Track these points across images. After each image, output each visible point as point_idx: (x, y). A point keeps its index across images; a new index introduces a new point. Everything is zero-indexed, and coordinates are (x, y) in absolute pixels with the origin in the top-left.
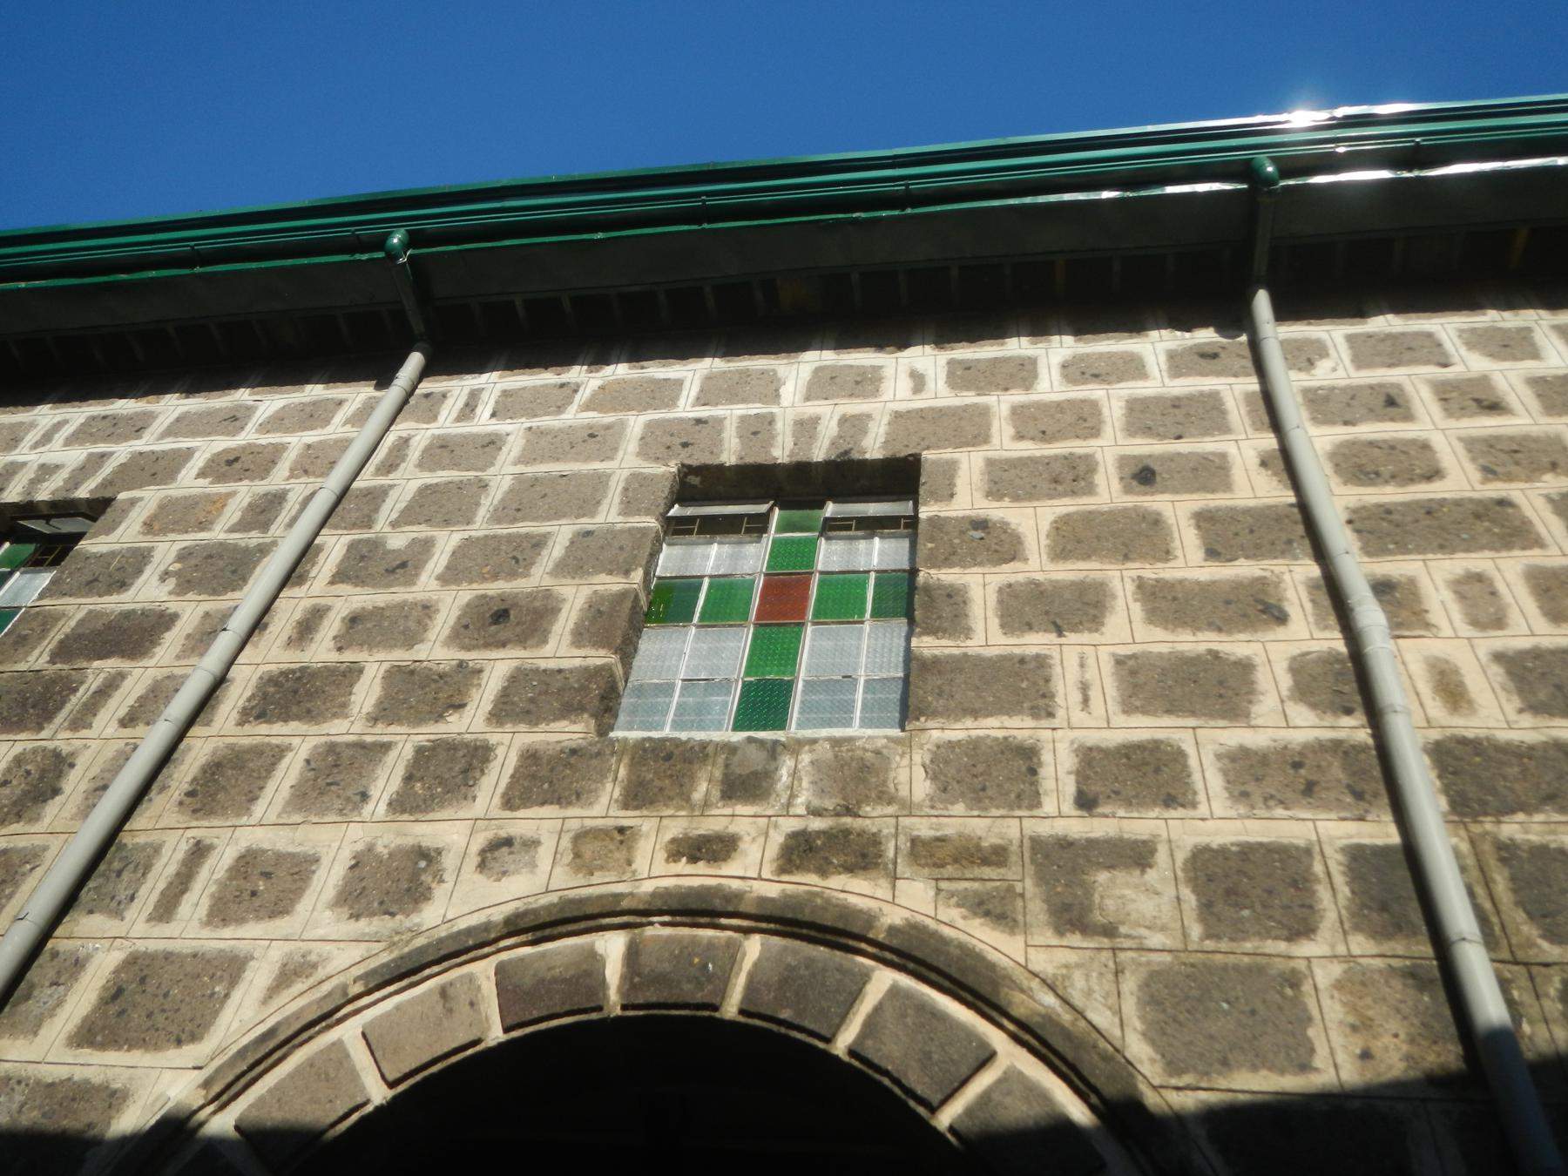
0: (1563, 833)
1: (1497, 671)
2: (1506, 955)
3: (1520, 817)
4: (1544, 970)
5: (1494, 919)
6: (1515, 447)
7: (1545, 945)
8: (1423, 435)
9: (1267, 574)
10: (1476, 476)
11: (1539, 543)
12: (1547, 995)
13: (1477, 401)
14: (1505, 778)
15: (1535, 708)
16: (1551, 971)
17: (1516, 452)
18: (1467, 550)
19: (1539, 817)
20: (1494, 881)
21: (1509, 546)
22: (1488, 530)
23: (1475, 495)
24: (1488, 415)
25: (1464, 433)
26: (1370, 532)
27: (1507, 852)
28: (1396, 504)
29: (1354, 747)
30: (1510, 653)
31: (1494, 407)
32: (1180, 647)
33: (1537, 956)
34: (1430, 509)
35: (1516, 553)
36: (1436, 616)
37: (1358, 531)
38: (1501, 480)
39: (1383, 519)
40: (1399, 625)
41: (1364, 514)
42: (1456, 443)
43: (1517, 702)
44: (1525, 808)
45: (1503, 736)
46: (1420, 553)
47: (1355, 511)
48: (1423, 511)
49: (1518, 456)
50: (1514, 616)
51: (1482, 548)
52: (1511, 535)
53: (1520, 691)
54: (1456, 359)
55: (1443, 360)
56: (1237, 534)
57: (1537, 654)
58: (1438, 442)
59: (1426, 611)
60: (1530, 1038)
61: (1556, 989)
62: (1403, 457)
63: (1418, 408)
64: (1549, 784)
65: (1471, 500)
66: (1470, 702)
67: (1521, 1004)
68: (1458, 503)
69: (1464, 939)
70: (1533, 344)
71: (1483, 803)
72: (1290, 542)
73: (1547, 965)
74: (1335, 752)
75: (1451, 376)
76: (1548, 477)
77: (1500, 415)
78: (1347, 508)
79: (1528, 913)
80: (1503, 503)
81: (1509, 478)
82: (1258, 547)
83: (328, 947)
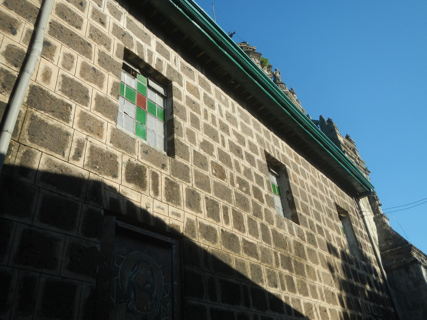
0: (49, 120)
1: (60, 79)
2: (17, 140)
3: (43, 112)
4: (24, 146)
5: (19, 131)
6: (101, 35)
7: (28, 141)
8: (83, 17)
9: (18, 20)
10: (88, 35)
11: (90, 58)
12: (20, 152)
13: (100, 19)
14: (45, 102)
15: (63, 91)
16: (25, 147)
17: (100, 36)
18: (74, 49)
19: (47, 114)
20: (26, 123)
21: (83, 55)
22: (81, 48)
23: (84, 39)
24: (100, 24)
25: (92, 24)
26: (54, 30)
27: (33, 118)
28: (65, 27)
29: (11, 75)
30: (67, 77)
31: (103, 23)
33: (24, 142)
34: (72, 34)
35: (84, 57)
36: (56, 58)
37: (51, 27)
38: (92, 39)
39: (59, 28)
40: (45, 55)
41: (55, 24)
42: (89, 24)
43: (60, 88)
44: (45, 111)
45: (51, 93)
46: (62, 42)
47: (53, 22)
48: (70, 34)
49: (100, 37)
50: (73, 70)
51: (77, 51)
52: (86, 52)
53: (63, 86)
54: (103, 7)
55: (100, 5)
56: (17, 4)
57: (72, 80)
58: (85, 21)
59: (54, 56)
60: (9, 159)
61: (23, 151)
62: (74, 18)
63: (86, 10)
64: (54, 108)
65: (83, 39)
66: (49, 82)
67: (13, 151)
68: (79, 38)
69: (7, 131)
70: (120, 17)
71: (36, 105)
72: (31, 17)
73: (25, 145)
74: (5, 73)
75: (99, 9)
76: (103, 46)
77: (103, 26)
78: (52, 20)
79: (29, 133)
80: (89, 44)
81: (94, 40)
82: (21, 11)
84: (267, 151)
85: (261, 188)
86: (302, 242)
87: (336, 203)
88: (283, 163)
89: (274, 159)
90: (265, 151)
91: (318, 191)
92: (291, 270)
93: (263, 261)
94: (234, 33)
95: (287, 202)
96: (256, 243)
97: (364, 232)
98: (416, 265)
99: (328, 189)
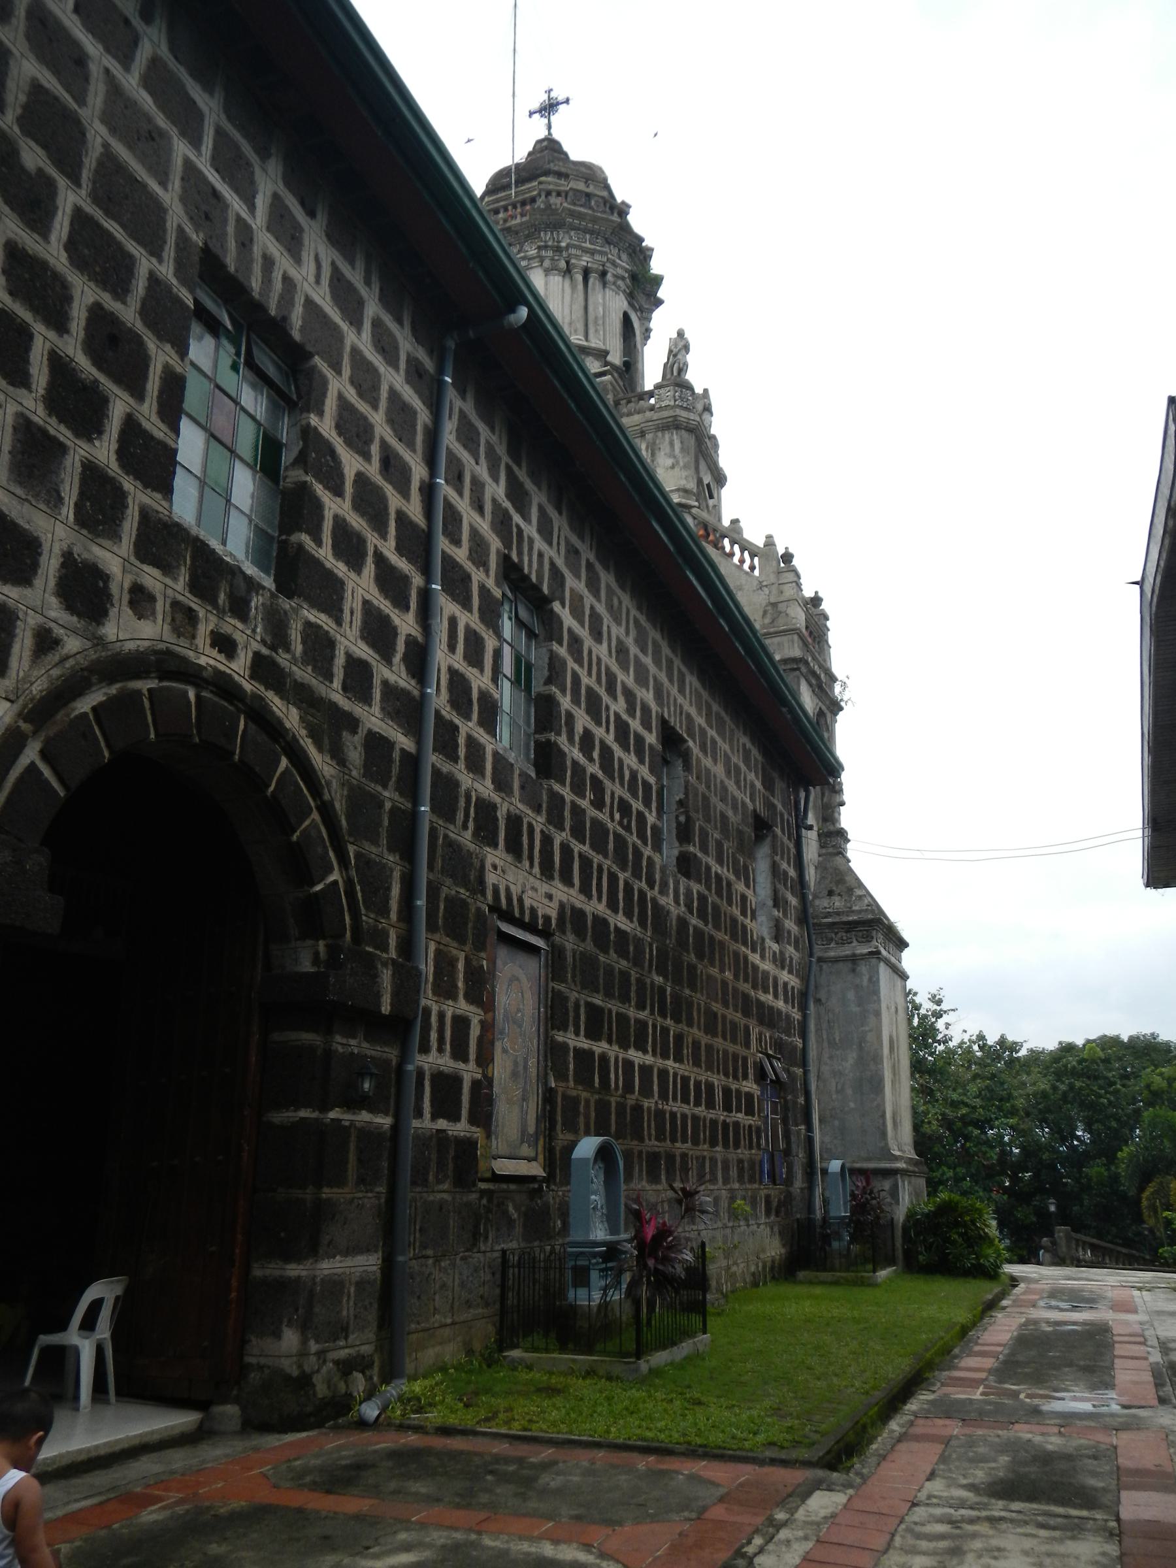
32: (382, 607)
83: (62, 631)
84: (666, 715)
85: (647, 814)
86: (688, 916)
87: (755, 810)
88: (685, 735)
89: (673, 728)
90: (662, 716)
91: (730, 789)
92: (666, 977)
93: (635, 964)
94: (567, 101)
95: (674, 825)
96: (629, 930)
97: (792, 873)
98: (874, 961)
99: (749, 778)
